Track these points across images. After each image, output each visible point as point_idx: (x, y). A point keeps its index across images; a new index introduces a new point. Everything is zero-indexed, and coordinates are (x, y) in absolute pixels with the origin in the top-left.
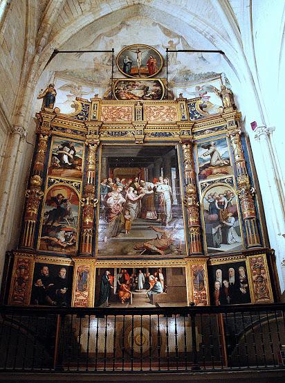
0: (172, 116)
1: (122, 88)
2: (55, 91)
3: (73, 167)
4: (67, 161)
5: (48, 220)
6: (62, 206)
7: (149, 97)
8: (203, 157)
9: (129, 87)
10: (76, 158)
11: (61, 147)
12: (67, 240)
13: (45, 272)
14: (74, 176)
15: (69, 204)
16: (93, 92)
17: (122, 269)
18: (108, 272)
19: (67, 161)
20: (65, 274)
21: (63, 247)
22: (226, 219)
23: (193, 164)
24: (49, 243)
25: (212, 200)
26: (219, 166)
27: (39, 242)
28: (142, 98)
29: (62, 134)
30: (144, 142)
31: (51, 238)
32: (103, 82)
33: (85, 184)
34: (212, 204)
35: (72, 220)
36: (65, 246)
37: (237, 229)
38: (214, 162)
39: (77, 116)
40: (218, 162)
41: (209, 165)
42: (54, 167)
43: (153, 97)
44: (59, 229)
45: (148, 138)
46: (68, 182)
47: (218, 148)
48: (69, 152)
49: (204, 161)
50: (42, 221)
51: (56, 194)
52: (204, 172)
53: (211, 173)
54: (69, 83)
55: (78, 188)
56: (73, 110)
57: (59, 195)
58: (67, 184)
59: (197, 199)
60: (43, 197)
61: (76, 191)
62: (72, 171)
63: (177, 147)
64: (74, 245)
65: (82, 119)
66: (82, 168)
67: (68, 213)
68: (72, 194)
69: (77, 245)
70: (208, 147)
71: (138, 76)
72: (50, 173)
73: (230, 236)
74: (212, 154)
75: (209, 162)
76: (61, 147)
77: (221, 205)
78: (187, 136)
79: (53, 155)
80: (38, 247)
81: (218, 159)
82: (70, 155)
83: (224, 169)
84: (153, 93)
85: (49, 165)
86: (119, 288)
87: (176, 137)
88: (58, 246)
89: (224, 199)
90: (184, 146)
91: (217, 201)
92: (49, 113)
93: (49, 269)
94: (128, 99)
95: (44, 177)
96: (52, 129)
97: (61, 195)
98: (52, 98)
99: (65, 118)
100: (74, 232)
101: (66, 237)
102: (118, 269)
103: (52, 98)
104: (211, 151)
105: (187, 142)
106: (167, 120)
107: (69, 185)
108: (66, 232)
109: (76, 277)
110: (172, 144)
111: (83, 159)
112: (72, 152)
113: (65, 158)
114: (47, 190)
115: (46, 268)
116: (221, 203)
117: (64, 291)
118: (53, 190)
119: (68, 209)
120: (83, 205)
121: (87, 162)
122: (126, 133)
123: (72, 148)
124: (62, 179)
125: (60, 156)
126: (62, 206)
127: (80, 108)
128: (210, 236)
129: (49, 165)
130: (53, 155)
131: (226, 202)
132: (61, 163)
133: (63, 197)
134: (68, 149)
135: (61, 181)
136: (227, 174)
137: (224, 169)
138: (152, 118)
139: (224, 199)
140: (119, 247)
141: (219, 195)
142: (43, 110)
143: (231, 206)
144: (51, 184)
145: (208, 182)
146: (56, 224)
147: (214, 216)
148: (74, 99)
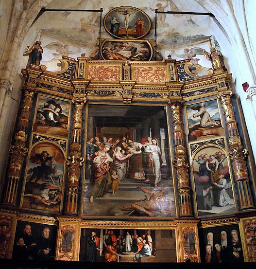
0: (161, 78)
1: (109, 49)
2: (41, 48)
3: (59, 125)
4: (52, 119)
5: (32, 178)
6: (47, 164)
7: (137, 57)
8: (192, 118)
9: (117, 48)
10: (61, 116)
11: (46, 104)
12: (51, 198)
13: (27, 231)
14: (59, 134)
15: (54, 162)
16: (79, 52)
17: (109, 230)
18: (94, 234)
19: (52, 119)
20: (48, 234)
21: (46, 206)
22: (218, 181)
23: (182, 125)
24: (33, 201)
25: (202, 162)
26: (209, 127)
27: (22, 199)
28: (130, 59)
29: (48, 91)
30: (133, 102)
31: (35, 196)
32: (90, 42)
33: (71, 142)
34: (202, 166)
35: (57, 178)
36: (49, 204)
37: (229, 191)
38: (204, 123)
39: (63, 74)
40: (209, 124)
41: (199, 126)
42: (39, 124)
43: (141, 59)
44: (43, 187)
45: (136, 98)
46: (53, 140)
47: (208, 110)
48: (55, 110)
49: (194, 122)
50: (25, 178)
51: (40, 151)
52: (194, 133)
53: (201, 135)
54: (56, 41)
55: (63, 146)
56: (59, 69)
57: (44, 152)
58: (52, 142)
59: (187, 160)
60: (27, 154)
61: (61, 149)
62: (58, 129)
63: (166, 108)
64: (59, 204)
65: (68, 77)
66: (68, 126)
67: (54, 171)
68: (57, 151)
69: (62, 204)
70: (198, 108)
71: (125, 37)
72: (35, 130)
73: (221, 198)
74: (202, 116)
75: (199, 123)
76: (46, 104)
77: (212, 166)
78: (175, 97)
79: (38, 112)
80: (21, 205)
81: (208, 121)
82: (55, 112)
83: (214, 131)
84: (141, 54)
85: (34, 122)
86: (105, 250)
87: (165, 98)
88: (42, 204)
89: (214, 161)
90: (173, 107)
91: (207, 163)
92: (35, 69)
93: (31, 229)
94: (115, 59)
95: (28, 134)
96: (38, 86)
97: (46, 152)
98: (38, 55)
99: (51, 75)
100: (59, 191)
101: (50, 195)
102: (104, 230)
103: (38, 55)
104: (201, 112)
105: (176, 103)
106: (155, 81)
107: (54, 143)
108: (51, 190)
109: (60, 237)
110: (161, 105)
111: (69, 117)
112: (58, 110)
113: (51, 116)
114: (31, 147)
115: (29, 227)
116: (212, 164)
117: (47, 251)
118: (38, 147)
119: (53, 166)
120: (68, 164)
121: (73, 120)
122: (113, 92)
123: (58, 106)
124: (48, 136)
125: (46, 114)
126: (47, 164)
127: (67, 66)
128: (201, 198)
129: (34, 122)
130: (38, 112)
131: (218, 163)
132: (45, 120)
133: (48, 155)
134: (54, 107)
135: (46, 138)
136: (217, 135)
137: (214, 131)
138: (140, 79)
139: (214, 161)
140: (105, 208)
141: (210, 156)
142: (29, 66)
143: (223, 168)
144: (35, 140)
145: (198, 144)
146: (40, 182)
147: (205, 178)
148: (60, 58)
